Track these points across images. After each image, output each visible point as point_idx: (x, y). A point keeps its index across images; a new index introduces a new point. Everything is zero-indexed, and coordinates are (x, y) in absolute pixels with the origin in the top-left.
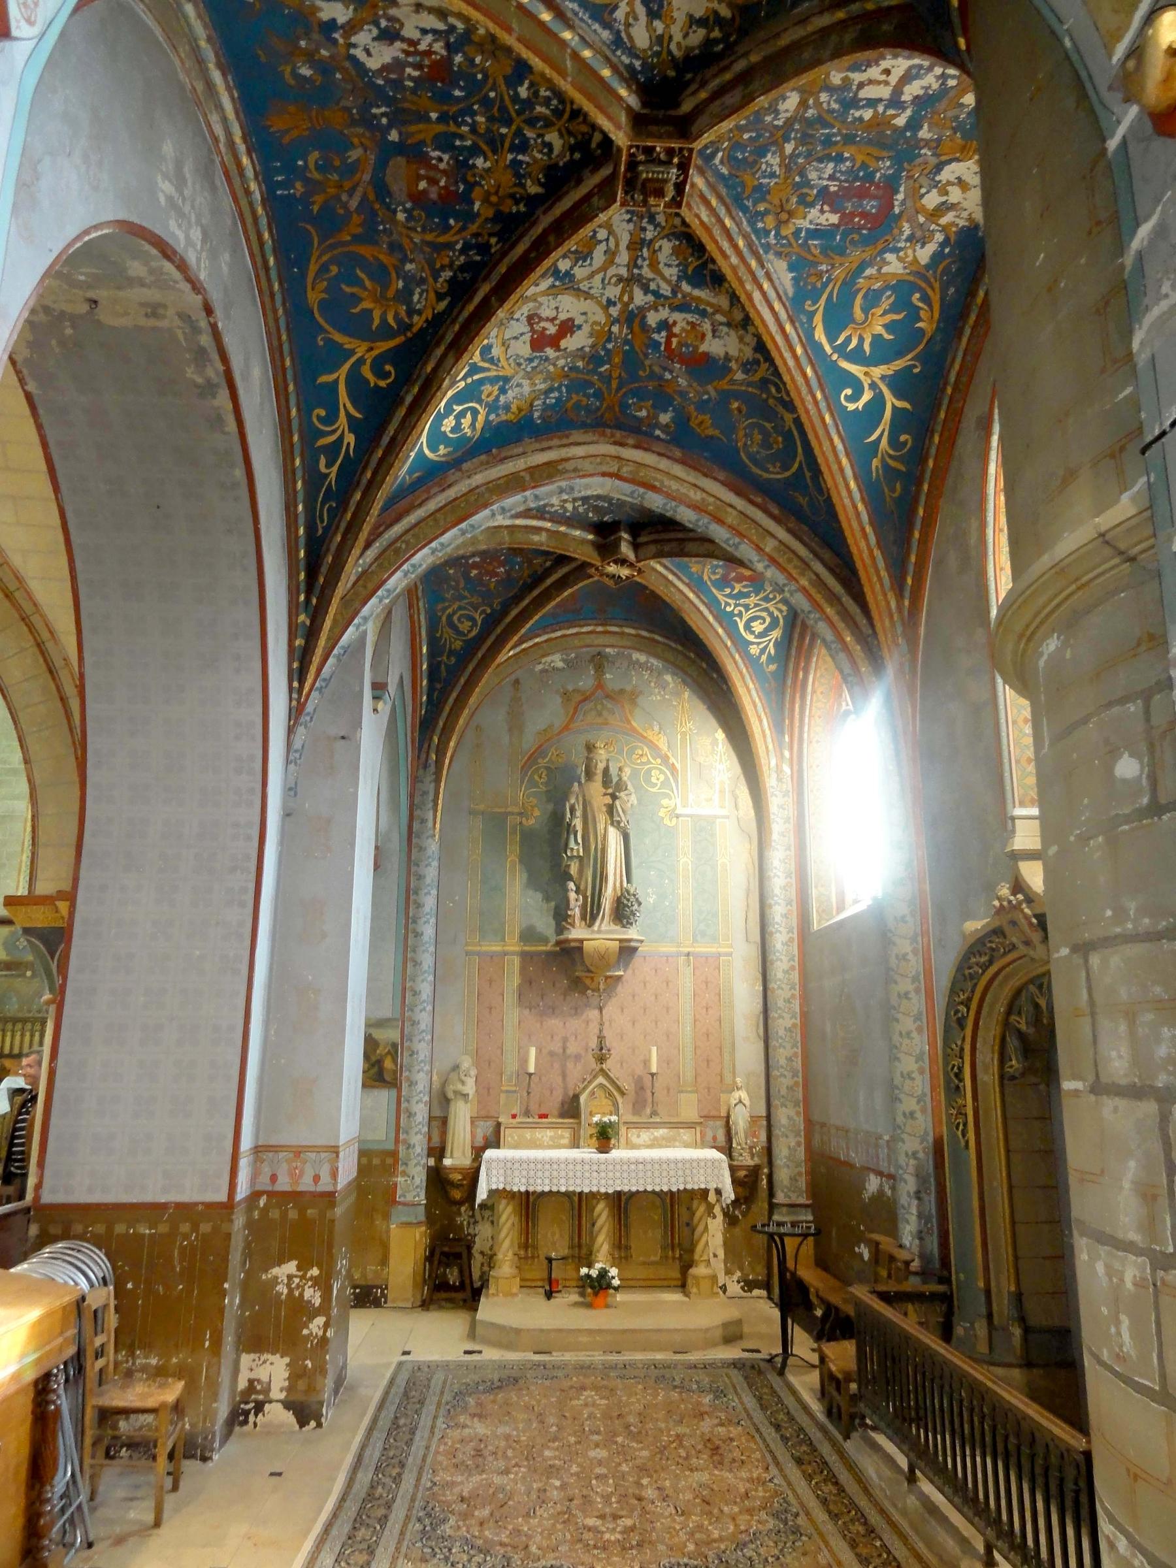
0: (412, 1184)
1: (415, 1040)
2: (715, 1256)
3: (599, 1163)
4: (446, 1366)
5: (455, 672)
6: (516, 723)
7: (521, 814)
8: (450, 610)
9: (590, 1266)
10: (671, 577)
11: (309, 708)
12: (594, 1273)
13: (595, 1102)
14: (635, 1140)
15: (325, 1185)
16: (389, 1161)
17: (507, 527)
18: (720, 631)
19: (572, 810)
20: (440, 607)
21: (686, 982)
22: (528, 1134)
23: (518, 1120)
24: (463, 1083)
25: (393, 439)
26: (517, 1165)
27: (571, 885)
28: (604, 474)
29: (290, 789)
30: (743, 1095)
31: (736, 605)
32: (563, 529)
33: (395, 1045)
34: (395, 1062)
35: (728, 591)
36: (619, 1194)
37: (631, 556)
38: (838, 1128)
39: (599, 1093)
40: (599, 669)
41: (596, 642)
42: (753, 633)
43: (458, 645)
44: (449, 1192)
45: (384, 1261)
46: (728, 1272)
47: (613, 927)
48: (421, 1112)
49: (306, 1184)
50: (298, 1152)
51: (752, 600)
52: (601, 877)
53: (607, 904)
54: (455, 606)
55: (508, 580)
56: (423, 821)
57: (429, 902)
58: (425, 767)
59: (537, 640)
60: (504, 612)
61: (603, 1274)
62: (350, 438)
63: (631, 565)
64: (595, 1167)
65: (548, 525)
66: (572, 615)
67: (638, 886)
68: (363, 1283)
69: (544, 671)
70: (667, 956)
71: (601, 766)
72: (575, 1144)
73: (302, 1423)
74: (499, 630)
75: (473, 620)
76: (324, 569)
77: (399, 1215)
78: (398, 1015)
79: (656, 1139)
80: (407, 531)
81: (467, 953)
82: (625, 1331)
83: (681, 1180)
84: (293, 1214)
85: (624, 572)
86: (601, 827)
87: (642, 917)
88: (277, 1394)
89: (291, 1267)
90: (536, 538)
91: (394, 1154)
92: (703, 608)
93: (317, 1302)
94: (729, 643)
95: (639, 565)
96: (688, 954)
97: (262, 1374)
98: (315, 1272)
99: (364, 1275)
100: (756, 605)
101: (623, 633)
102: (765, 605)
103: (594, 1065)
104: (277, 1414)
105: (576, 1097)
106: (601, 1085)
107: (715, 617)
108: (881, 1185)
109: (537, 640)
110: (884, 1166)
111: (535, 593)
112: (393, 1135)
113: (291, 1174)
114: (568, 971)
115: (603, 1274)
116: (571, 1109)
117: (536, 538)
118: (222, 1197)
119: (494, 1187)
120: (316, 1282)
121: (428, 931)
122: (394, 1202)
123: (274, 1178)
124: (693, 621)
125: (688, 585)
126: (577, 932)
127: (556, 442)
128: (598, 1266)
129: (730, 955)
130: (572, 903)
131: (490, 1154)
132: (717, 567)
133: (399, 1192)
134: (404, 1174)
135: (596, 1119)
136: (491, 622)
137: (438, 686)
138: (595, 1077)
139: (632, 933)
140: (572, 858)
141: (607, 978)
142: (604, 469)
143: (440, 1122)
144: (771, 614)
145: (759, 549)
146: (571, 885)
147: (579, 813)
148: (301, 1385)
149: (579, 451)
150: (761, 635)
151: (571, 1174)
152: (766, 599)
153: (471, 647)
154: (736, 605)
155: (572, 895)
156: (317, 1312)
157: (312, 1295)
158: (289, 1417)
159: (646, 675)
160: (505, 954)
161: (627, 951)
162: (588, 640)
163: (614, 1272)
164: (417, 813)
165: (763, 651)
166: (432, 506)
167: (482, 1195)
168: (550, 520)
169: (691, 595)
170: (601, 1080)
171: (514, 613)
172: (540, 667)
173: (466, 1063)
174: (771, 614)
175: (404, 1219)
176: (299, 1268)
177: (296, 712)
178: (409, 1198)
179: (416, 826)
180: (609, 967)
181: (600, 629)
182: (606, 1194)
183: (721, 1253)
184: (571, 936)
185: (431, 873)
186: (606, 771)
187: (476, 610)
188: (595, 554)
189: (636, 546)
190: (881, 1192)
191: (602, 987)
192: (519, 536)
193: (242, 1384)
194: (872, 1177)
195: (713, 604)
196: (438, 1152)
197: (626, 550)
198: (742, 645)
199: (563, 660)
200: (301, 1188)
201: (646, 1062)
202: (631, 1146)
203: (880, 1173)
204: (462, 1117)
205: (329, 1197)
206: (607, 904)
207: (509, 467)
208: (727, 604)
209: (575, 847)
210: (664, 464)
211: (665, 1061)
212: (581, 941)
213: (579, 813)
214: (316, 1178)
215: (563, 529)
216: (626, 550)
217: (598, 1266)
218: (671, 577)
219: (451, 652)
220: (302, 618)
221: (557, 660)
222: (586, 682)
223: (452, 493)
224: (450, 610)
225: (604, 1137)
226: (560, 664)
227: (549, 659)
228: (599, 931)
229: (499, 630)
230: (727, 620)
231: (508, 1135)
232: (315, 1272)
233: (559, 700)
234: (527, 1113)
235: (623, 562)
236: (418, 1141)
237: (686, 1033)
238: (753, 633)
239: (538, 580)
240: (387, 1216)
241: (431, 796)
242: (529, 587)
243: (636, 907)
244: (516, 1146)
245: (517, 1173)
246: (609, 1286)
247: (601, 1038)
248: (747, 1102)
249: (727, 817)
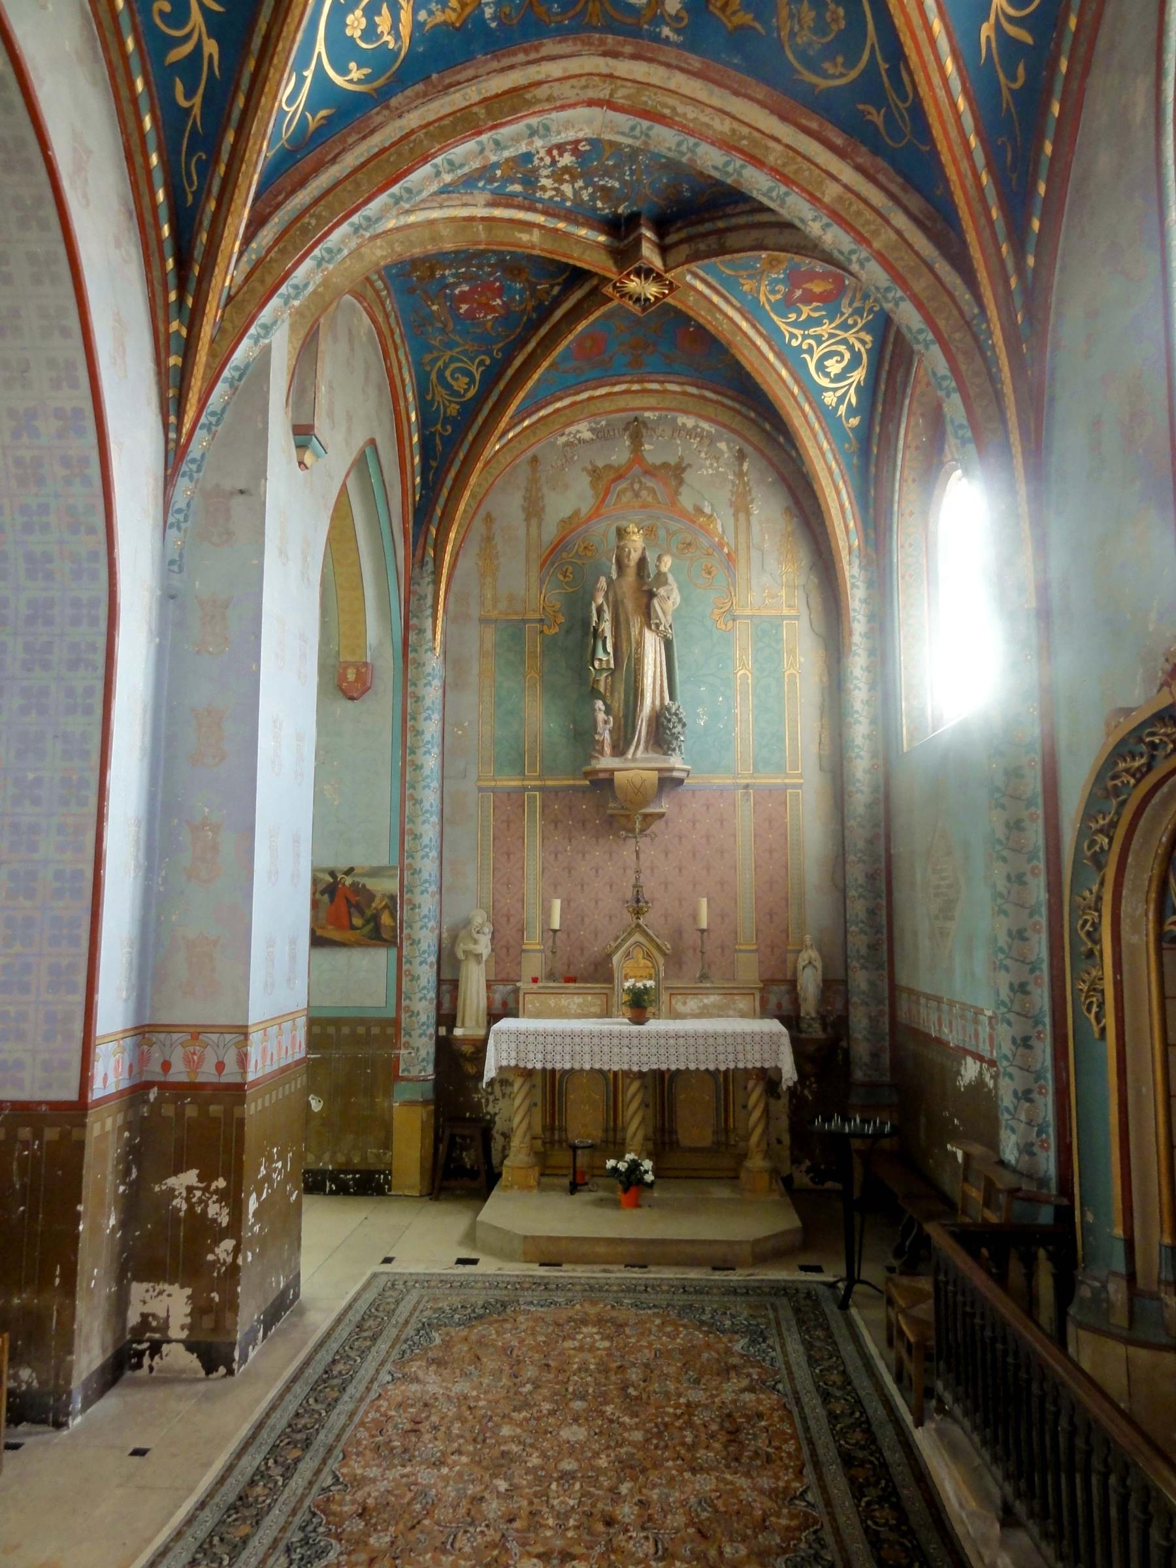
0: (418, 1057)
1: (418, 890)
2: (779, 1141)
3: (630, 1036)
4: (425, 1281)
5: (452, 443)
6: (533, 509)
7: (541, 621)
8: (440, 363)
9: (620, 1157)
10: (716, 299)
11: (196, 449)
12: (622, 1166)
13: (630, 963)
14: (680, 1007)
15: (230, 1075)
16: (390, 1031)
17: (483, 219)
18: (784, 373)
19: (600, 611)
20: (428, 357)
21: (744, 819)
22: (552, 1001)
23: (540, 984)
24: (476, 942)
25: (266, 38)
26: (531, 1039)
27: (600, 704)
28: (591, 103)
29: (172, 562)
30: (813, 954)
31: (805, 337)
32: (561, 225)
33: (392, 898)
34: (394, 917)
35: (793, 316)
36: (659, 1075)
37: (657, 263)
38: (928, 997)
39: (638, 954)
40: (637, 440)
41: (632, 404)
42: (827, 375)
43: (453, 409)
45: (387, 1144)
46: (795, 1161)
47: (651, 755)
48: (426, 974)
49: (207, 1074)
50: (196, 1033)
51: (825, 329)
52: (635, 692)
53: (642, 727)
54: (447, 358)
55: (507, 316)
56: (421, 631)
57: (431, 728)
58: (422, 564)
59: (558, 405)
60: (508, 360)
61: (634, 1166)
62: (211, 47)
63: (659, 278)
64: (626, 1042)
65: (540, 219)
66: (596, 364)
67: (682, 706)
68: (363, 1167)
69: (568, 444)
70: (722, 790)
71: (635, 556)
72: (606, 1013)
73: (210, 1368)
74: (501, 385)
75: (469, 374)
76: (198, 253)
77: (403, 1093)
78: (396, 862)
79: (705, 1006)
80: (316, 202)
81: (480, 789)
82: (652, 1242)
83: (731, 1057)
84: (191, 1112)
85: (651, 290)
86: (635, 632)
87: (685, 739)
88: (175, 1332)
89: (190, 1177)
90: (525, 237)
91: (396, 1023)
92: (759, 342)
93: (224, 1220)
94: (796, 390)
95: (668, 276)
96: (747, 786)
97: (157, 1307)
98: (221, 1183)
99: (364, 1159)
100: (832, 336)
101: (665, 391)
102: (842, 335)
103: (628, 918)
104: (176, 1356)
105: (609, 956)
106: (638, 944)
107: (778, 355)
108: (981, 1073)
109: (558, 405)
110: (984, 1049)
111: (543, 331)
112: (393, 1001)
113: (188, 1061)
114: (603, 809)
115: (634, 1166)
116: (599, 972)
117: (525, 237)
118: (72, 1095)
119: (504, 1063)
120: (223, 1196)
121: (431, 763)
122: (398, 1078)
123: (166, 1066)
124: (748, 359)
125: (738, 310)
126: (606, 762)
127: (521, 57)
128: (629, 1157)
129: (800, 786)
130: (600, 724)
131: (505, 1024)
132: (777, 281)
133: (402, 1066)
134: (407, 1045)
135: (627, 985)
136: (492, 376)
137: (434, 464)
138: (630, 934)
139: (676, 761)
140: (601, 670)
141: (646, 816)
142: (591, 94)
143: (448, 985)
144: (851, 348)
145: (814, 199)
146: (600, 704)
147: (607, 616)
148: (207, 1322)
149: (554, 69)
150: (840, 377)
151: (596, 1049)
152: (844, 327)
153: (470, 409)
154: (805, 337)
155: (601, 716)
156: (223, 1234)
157: (218, 1212)
158: (192, 1362)
159: (695, 442)
160: (525, 789)
161: (668, 782)
162: (622, 402)
163: (647, 1164)
164: (413, 621)
165: (841, 400)
166: (350, 160)
168: (544, 213)
169: (744, 325)
170: (637, 937)
171: (517, 362)
172: (564, 439)
173: (479, 918)
174: (851, 348)
175: (407, 1097)
176: (201, 1178)
177: (175, 456)
178: (414, 1072)
179: (412, 637)
180: (646, 803)
181: (636, 387)
182: (640, 1072)
183: (786, 1139)
184: (598, 767)
185: (432, 693)
186: (642, 562)
187: (472, 360)
188: (610, 263)
189: (664, 250)
190: (980, 1081)
191: (638, 826)
192: (500, 234)
193: (133, 1318)
194: (969, 1060)
195: (773, 337)
196: (447, 1018)
197: (649, 253)
198: (813, 393)
199: (592, 430)
200: (201, 1079)
201: (695, 917)
202: (676, 1015)
203: (979, 1057)
205: (237, 1091)
206: (642, 727)
207: (456, 100)
208: (793, 336)
209: (604, 656)
210: (679, 81)
211: (719, 915)
212: (612, 771)
213: (607, 616)
214: (220, 1066)
215: (561, 225)
216: (649, 253)
217: (629, 1157)
218: (716, 299)
219: (447, 420)
220: (175, 326)
221: (583, 430)
222: (620, 454)
223: (376, 141)
224: (440, 363)
225: (640, 1006)
226: (587, 435)
227: (573, 429)
228: (634, 759)
229: (501, 385)
230: (792, 358)
231: (530, 1003)
232: (221, 1183)
233: (586, 479)
234: (551, 976)
235: (646, 273)
236: (423, 1008)
237: (746, 880)
238: (827, 375)
239: (544, 312)
240: (388, 1093)
241: (429, 601)
242: (535, 326)
243: (679, 728)
244: (538, 1015)
245: (531, 1047)
246: (641, 1182)
247: (637, 887)
248: (819, 964)
249: (797, 618)
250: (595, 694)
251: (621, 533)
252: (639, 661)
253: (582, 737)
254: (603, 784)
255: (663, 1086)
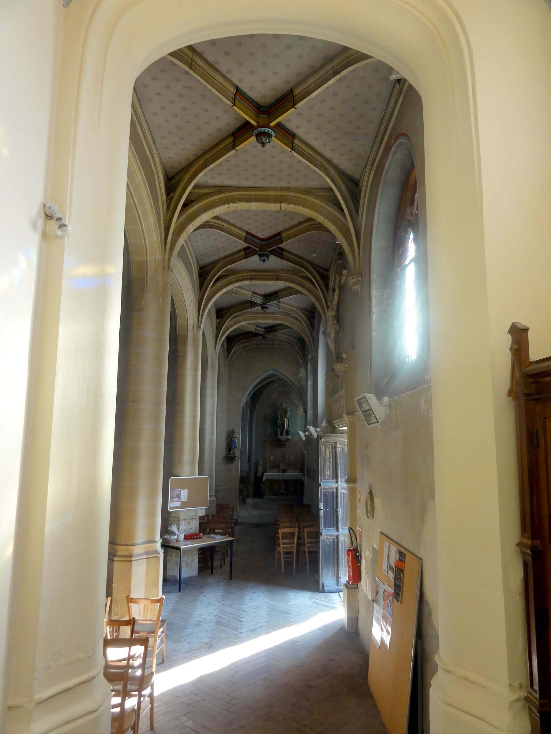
0: (252, 479)
44: (259, 480)
48: (253, 466)
72: (279, 472)
121: (254, 436)
126: (280, 437)
139: (289, 437)
143: (256, 469)
161: (288, 440)
167: (264, 479)
196: (256, 473)
204: (260, 468)
209: (279, 421)
221: (276, 386)
225: (284, 471)
236: (253, 471)
250: (278, 427)
251: (282, 404)
252: (284, 422)
253: (276, 433)
254: (279, 440)
255: (286, 482)
